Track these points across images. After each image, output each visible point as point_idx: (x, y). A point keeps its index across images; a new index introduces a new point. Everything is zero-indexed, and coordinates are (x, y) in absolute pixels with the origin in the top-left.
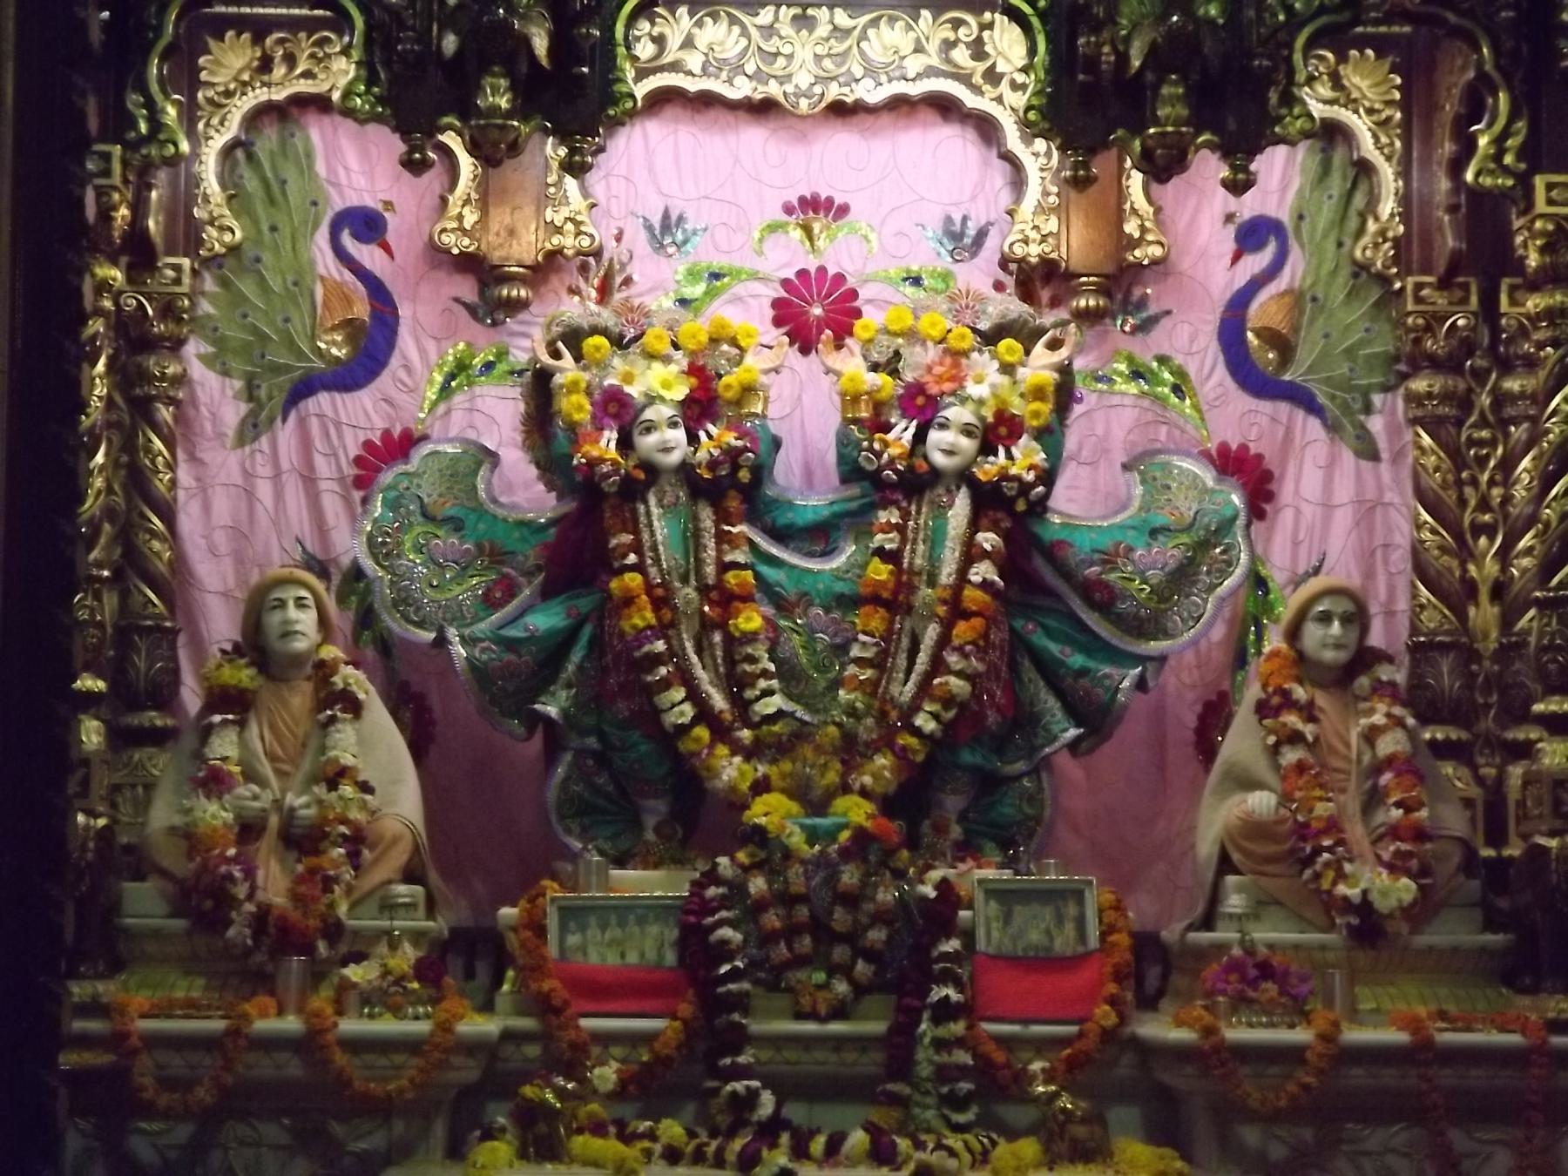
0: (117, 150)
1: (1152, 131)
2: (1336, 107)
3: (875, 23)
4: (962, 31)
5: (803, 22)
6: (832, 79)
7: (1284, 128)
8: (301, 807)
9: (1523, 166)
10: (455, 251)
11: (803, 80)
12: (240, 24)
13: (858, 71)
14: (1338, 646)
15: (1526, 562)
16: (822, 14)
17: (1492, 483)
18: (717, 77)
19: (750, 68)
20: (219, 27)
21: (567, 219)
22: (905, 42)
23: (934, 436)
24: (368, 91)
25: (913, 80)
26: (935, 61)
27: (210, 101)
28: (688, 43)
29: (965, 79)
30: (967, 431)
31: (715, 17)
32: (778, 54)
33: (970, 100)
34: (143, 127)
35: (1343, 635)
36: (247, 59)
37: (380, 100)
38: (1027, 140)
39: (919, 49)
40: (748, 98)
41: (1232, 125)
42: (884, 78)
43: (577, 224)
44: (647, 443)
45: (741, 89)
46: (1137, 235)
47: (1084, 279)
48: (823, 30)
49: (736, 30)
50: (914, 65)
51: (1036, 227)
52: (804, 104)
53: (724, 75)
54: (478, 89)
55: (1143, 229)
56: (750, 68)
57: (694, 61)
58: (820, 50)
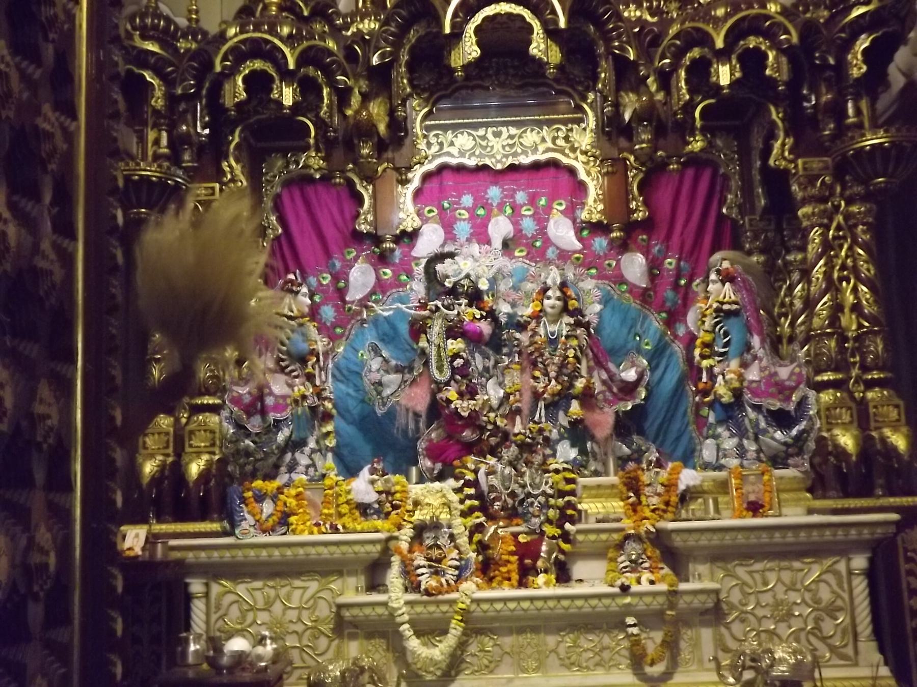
0: (217, 186)
1: (637, 147)
3: (525, 132)
4: (561, 134)
5: (497, 135)
9: (791, 156)
12: (277, 150)
13: (519, 151)
15: (803, 328)
16: (504, 129)
17: (786, 296)
19: (477, 153)
20: (268, 152)
22: (538, 140)
26: (552, 146)
27: (267, 180)
28: (452, 144)
29: (562, 152)
31: (462, 133)
32: (488, 146)
33: (565, 160)
34: (229, 176)
38: (588, 174)
39: (543, 140)
48: (505, 135)
49: (471, 138)
50: (541, 148)
53: (467, 156)
54: (359, 148)
55: (637, 206)
56: (477, 153)
58: (505, 143)
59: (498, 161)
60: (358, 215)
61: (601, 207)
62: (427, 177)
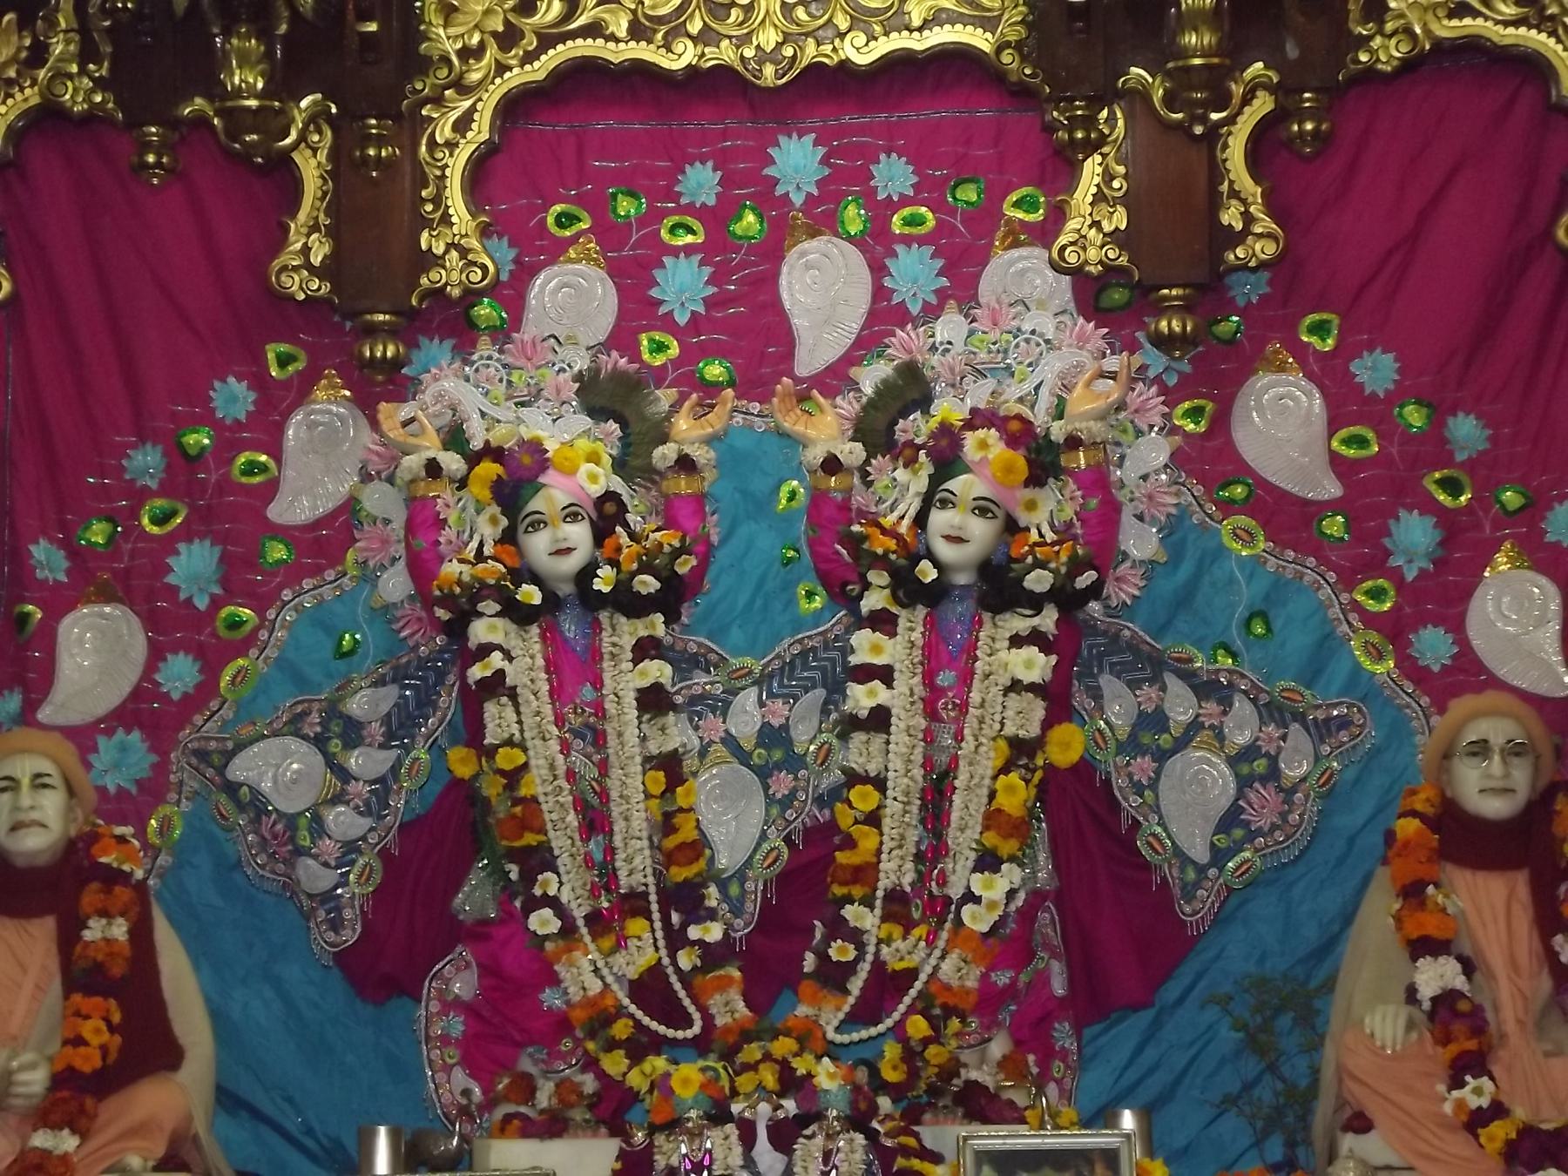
2: (1522, 30)
6: (807, 35)
7: (1371, 52)
8: (22, 1068)
10: (301, 297)
11: (768, 38)
13: (842, 22)
14: (1508, 791)
18: (650, 42)
19: (695, 27)
21: (449, 246)
23: (939, 519)
24: (83, 71)
25: (920, 29)
30: (982, 509)
35: (1507, 775)
36: (12, 51)
37: (100, 84)
40: (690, 65)
41: (1292, 51)
42: (878, 28)
43: (464, 252)
44: (538, 545)
45: (682, 57)
46: (1239, 226)
47: (1166, 291)
51: (1096, 224)
52: (769, 70)
53: (659, 36)
55: (1248, 219)
57: (620, 25)
59: (762, 56)
60: (279, 239)
61: (1120, 219)
62: (514, 107)
